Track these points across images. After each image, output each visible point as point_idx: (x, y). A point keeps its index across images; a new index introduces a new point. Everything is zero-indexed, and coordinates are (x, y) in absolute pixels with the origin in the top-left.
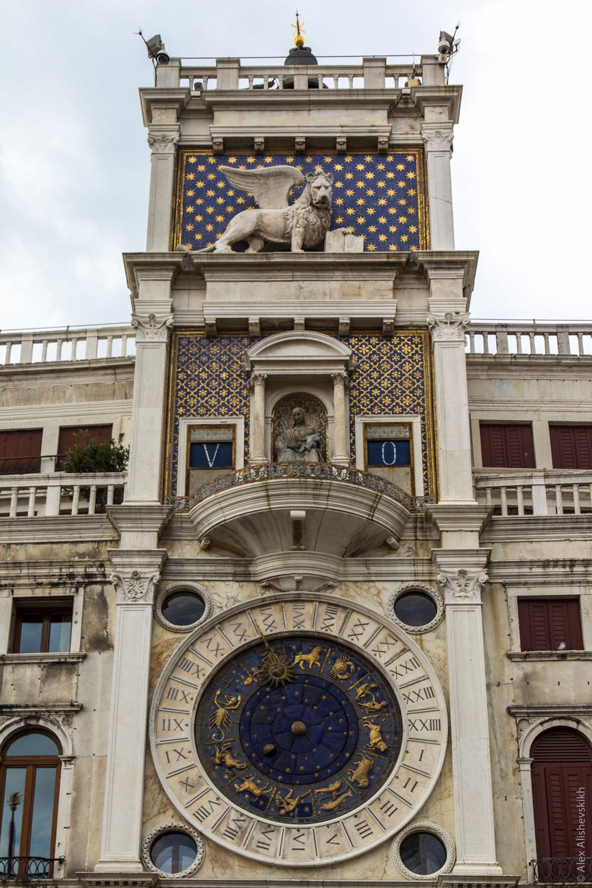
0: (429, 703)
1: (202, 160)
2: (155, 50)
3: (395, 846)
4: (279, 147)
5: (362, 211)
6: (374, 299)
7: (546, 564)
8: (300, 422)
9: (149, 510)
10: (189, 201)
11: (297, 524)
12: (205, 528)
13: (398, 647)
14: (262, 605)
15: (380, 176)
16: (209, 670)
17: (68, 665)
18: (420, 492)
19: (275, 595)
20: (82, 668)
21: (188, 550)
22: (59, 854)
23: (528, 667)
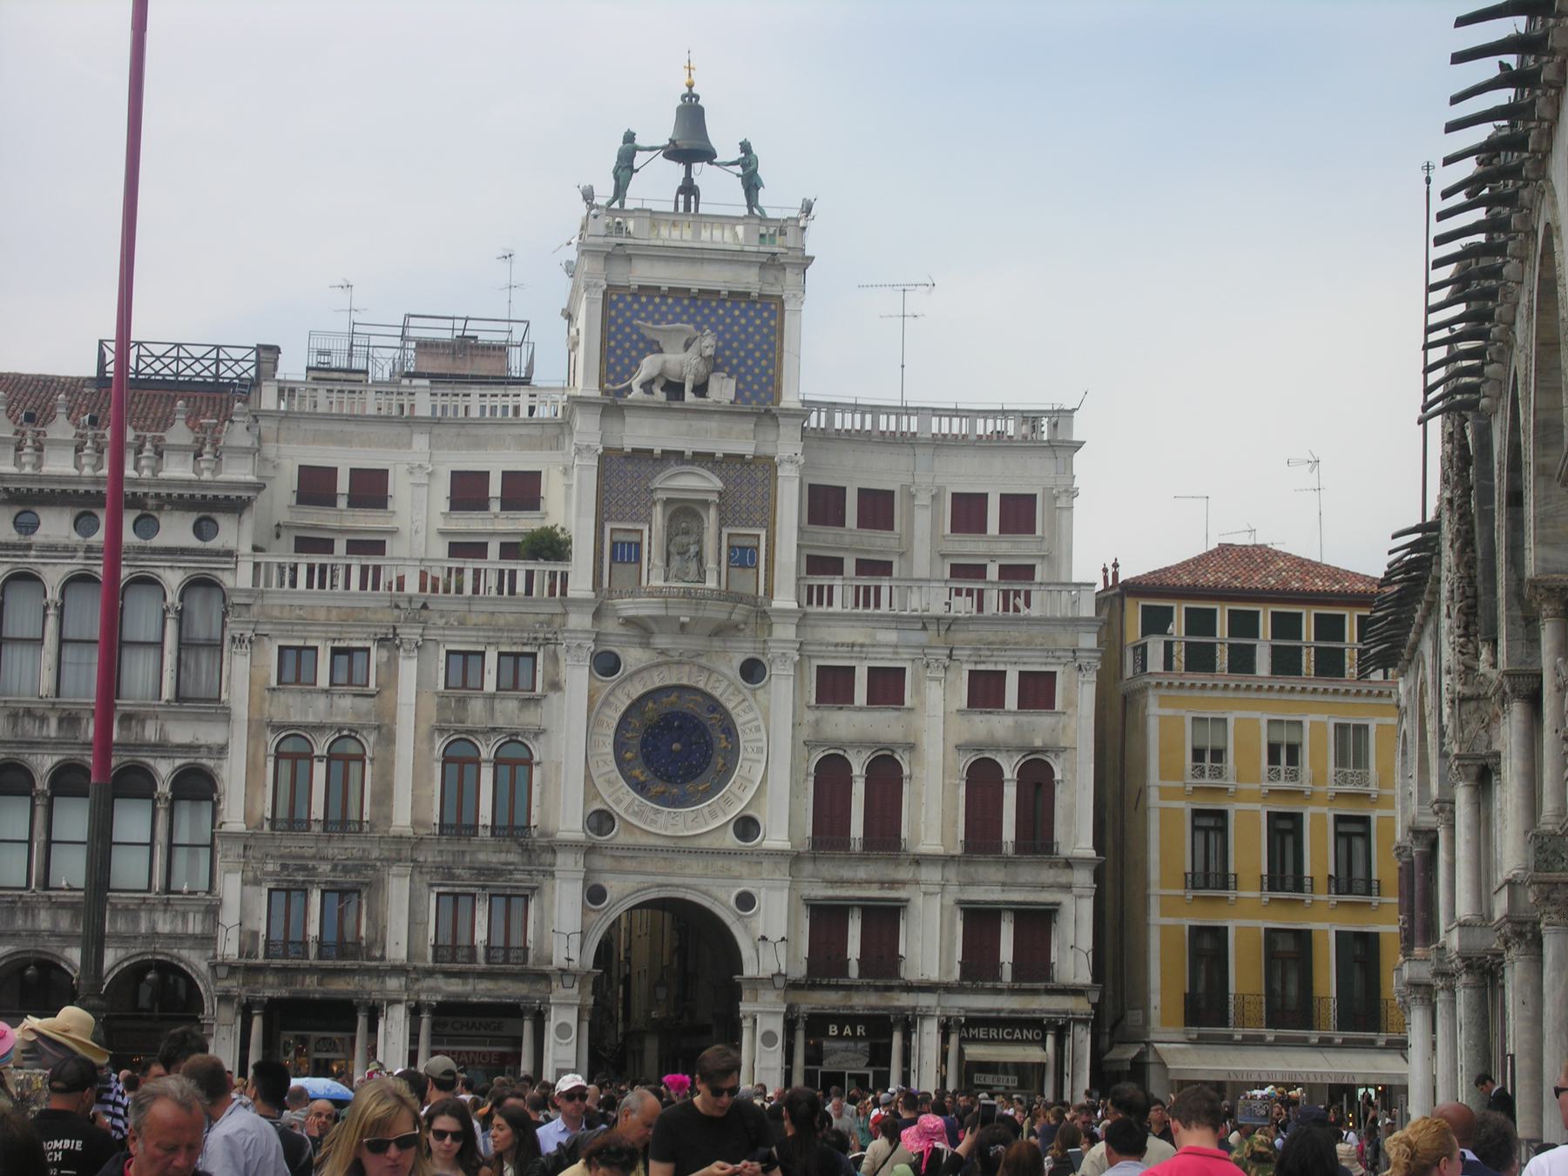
0: (757, 736)
1: (621, 298)
2: (588, 195)
3: (731, 826)
4: (678, 293)
5: (736, 354)
6: (739, 441)
7: (836, 645)
8: (686, 533)
9: (588, 601)
10: (612, 337)
11: (683, 625)
12: (625, 613)
13: (741, 698)
14: (658, 665)
15: (750, 322)
16: (623, 708)
17: (536, 701)
18: (761, 592)
19: (666, 660)
20: (544, 703)
21: (611, 626)
22: (533, 823)
23: (818, 713)
